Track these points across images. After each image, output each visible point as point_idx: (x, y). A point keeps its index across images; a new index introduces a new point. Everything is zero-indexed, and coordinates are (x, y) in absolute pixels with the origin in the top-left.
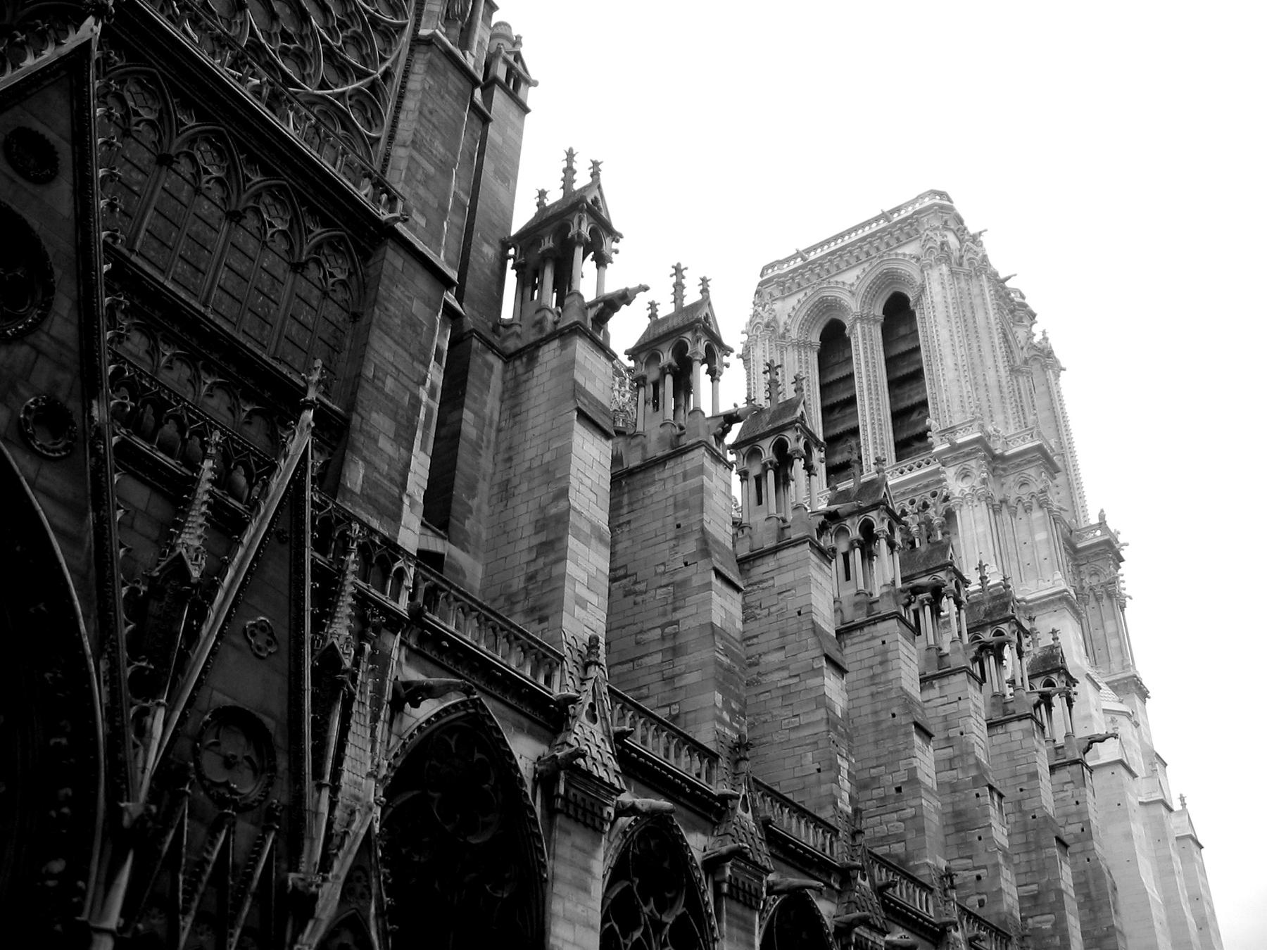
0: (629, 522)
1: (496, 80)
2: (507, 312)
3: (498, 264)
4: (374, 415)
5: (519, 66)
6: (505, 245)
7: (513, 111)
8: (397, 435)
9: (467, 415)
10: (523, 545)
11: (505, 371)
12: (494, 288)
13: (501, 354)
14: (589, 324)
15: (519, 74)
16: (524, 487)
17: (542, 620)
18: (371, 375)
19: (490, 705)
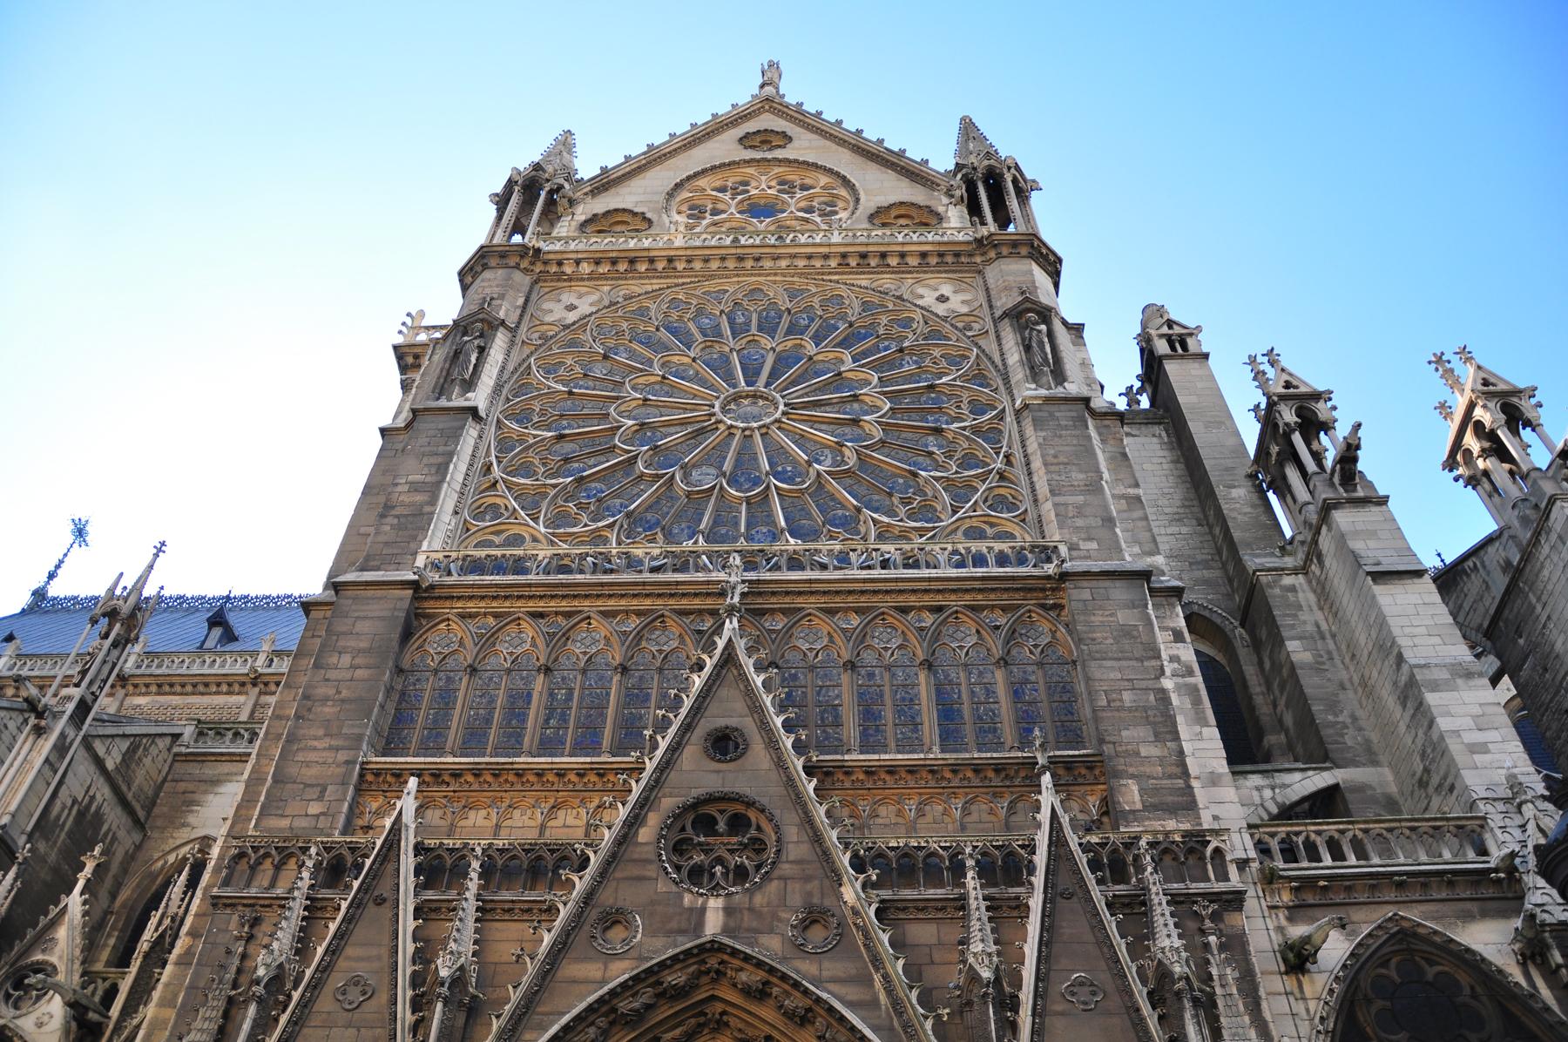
0: (1549, 618)
1: (1161, 359)
2: (1288, 533)
3: (1255, 497)
4: (1124, 733)
5: (1177, 330)
6: (1253, 477)
7: (1192, 367)
8: (1156, 735)
9: (1292, 645)
10: (1402, 727)
11: (1310, 582)
12: (1263, 518)
13: (1295, 571)
14: (1341, 490)
15: (1180, 335)
16: (1375, 674)
17: (1452, 788)
18: (1105, 703)
19: (1413, 914)
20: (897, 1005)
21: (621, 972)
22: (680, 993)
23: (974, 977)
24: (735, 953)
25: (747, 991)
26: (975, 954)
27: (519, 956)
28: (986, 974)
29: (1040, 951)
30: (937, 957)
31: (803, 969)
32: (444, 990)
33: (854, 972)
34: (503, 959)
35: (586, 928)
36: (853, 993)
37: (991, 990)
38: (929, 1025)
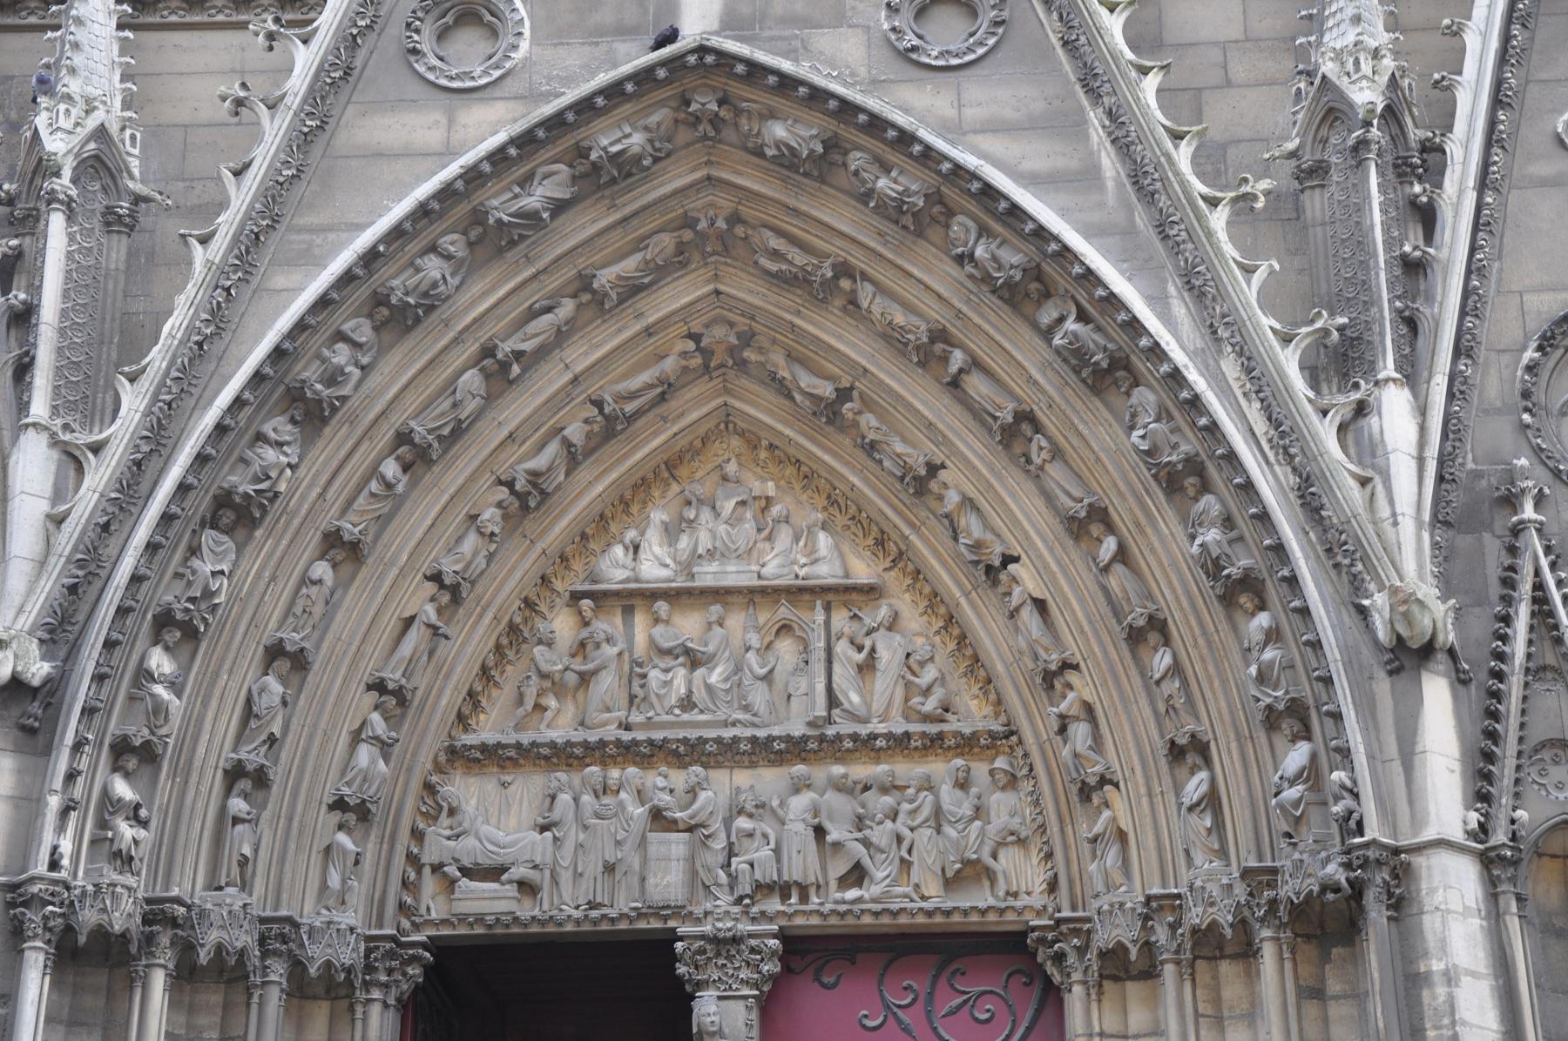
20: (1145, 180)
21: (489, 128)
22: (625, 169)
23: (1332, 110)
24: (756, 71)
25: (787, 162)
26: (1338, 55)
27: (239, 102)
28: (1366, 95)
29: (1506, 38)
30: (1239, 71)
31: (913, 106)
32: (64, 183)
33: (1039, 106)
34: (205, 115)
35: (395, 29)
36: (1039, 154)
37: (1375, 132)
38: (1219, 220)
